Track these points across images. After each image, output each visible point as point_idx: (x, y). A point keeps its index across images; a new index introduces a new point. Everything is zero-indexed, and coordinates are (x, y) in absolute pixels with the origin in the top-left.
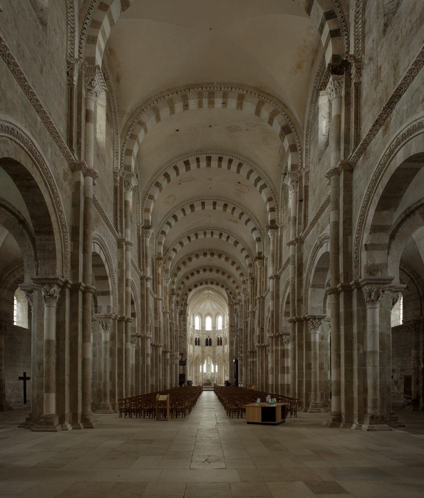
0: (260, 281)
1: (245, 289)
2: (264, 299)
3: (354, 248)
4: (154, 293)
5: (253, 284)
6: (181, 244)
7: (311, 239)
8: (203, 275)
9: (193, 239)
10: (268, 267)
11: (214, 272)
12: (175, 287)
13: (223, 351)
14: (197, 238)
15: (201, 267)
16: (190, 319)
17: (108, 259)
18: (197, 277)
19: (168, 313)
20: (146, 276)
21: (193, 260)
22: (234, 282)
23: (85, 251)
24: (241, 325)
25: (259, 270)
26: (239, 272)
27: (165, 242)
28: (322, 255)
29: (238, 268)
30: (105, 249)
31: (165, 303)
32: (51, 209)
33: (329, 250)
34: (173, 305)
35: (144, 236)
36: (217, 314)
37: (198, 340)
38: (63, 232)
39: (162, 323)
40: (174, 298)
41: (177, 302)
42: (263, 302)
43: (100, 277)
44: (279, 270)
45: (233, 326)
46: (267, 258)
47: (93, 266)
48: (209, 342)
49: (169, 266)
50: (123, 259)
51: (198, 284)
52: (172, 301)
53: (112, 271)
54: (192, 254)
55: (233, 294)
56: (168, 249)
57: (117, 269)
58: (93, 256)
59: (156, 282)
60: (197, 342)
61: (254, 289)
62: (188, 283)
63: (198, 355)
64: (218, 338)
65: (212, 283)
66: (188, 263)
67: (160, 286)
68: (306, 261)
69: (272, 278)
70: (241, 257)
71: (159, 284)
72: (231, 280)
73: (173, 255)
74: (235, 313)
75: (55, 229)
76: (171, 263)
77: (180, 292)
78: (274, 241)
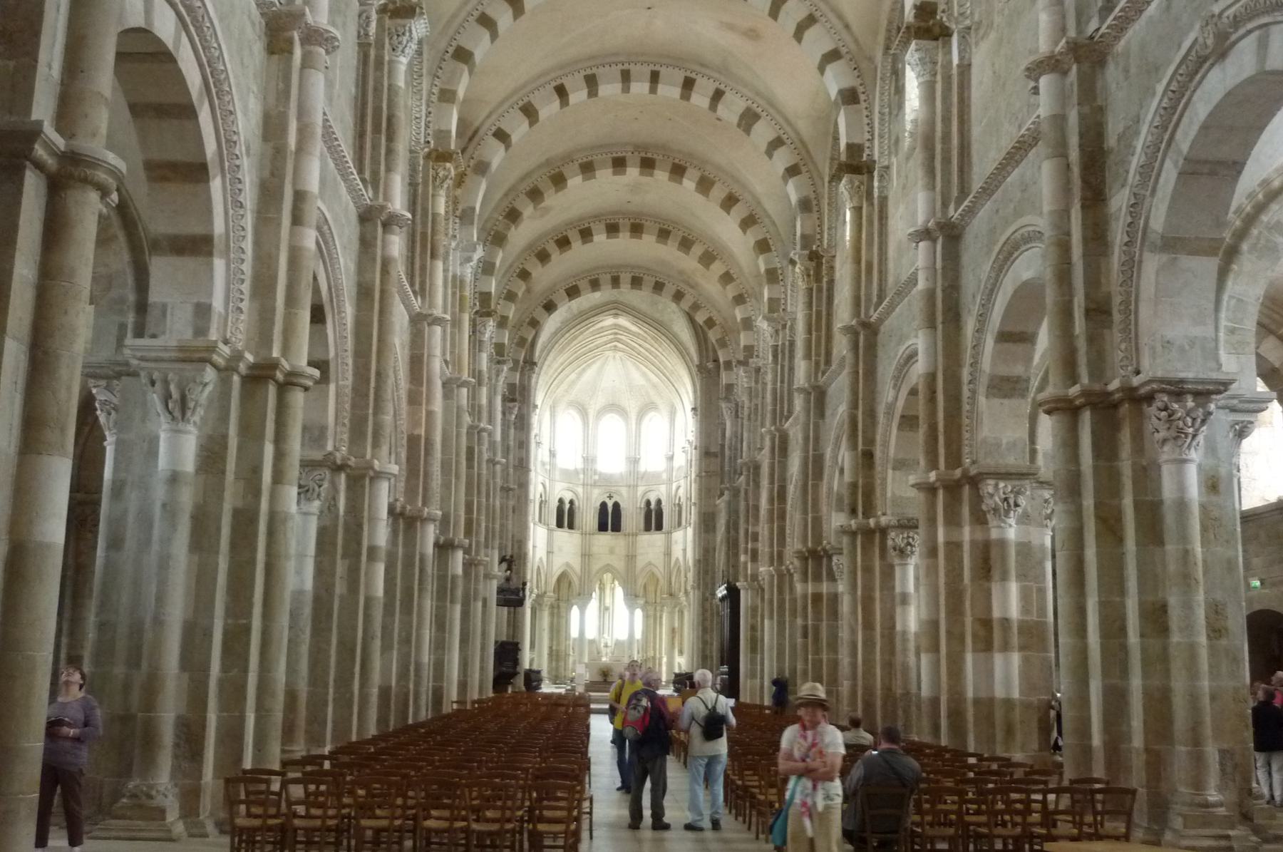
0: (857, 261)
4: (414, 292)
5: (818, 279)
6: (530, 112)
8: (604, 248)
9: (578, 96)
10: (891, 203)
11: (649, 239)
13: (668, 553)
14: (593, 92)
15: (597, 217)
16: (540, 422)
18: (580, 255)
19: (464, 384)
20: (383, 208)
21: (570, 182)
22: (727, 278)
26: (752, 237)
28: (1229, 94)
30: (199, 29)
31: (453, 345)
34: (484, 358)
35: (387, 46)
36: (647, 407)
37: (567, 506)
41: (499, 348)
42: (872, 348)
44: (959, 202)
45: (715, 455)
46: (887, 167)
48: (609, 519)
49: (479, 195)
52: (481, 342)
53: (232, 143)
54: (568, 158)
56: (476, 132)
57: (256, 145)
59: (424, 246)
60: (566, 517)
61: (819, 299)
62: (544, 276)
63: (567, 564)
64: (648, 503)
65: (636, 282)
66: (552, 199)
67: (440, 265)
71: (433, 256)
72: (718, 268)
73: (496, 155)
74: (727, 399)
76: (483, 186)
77: (511, 311)
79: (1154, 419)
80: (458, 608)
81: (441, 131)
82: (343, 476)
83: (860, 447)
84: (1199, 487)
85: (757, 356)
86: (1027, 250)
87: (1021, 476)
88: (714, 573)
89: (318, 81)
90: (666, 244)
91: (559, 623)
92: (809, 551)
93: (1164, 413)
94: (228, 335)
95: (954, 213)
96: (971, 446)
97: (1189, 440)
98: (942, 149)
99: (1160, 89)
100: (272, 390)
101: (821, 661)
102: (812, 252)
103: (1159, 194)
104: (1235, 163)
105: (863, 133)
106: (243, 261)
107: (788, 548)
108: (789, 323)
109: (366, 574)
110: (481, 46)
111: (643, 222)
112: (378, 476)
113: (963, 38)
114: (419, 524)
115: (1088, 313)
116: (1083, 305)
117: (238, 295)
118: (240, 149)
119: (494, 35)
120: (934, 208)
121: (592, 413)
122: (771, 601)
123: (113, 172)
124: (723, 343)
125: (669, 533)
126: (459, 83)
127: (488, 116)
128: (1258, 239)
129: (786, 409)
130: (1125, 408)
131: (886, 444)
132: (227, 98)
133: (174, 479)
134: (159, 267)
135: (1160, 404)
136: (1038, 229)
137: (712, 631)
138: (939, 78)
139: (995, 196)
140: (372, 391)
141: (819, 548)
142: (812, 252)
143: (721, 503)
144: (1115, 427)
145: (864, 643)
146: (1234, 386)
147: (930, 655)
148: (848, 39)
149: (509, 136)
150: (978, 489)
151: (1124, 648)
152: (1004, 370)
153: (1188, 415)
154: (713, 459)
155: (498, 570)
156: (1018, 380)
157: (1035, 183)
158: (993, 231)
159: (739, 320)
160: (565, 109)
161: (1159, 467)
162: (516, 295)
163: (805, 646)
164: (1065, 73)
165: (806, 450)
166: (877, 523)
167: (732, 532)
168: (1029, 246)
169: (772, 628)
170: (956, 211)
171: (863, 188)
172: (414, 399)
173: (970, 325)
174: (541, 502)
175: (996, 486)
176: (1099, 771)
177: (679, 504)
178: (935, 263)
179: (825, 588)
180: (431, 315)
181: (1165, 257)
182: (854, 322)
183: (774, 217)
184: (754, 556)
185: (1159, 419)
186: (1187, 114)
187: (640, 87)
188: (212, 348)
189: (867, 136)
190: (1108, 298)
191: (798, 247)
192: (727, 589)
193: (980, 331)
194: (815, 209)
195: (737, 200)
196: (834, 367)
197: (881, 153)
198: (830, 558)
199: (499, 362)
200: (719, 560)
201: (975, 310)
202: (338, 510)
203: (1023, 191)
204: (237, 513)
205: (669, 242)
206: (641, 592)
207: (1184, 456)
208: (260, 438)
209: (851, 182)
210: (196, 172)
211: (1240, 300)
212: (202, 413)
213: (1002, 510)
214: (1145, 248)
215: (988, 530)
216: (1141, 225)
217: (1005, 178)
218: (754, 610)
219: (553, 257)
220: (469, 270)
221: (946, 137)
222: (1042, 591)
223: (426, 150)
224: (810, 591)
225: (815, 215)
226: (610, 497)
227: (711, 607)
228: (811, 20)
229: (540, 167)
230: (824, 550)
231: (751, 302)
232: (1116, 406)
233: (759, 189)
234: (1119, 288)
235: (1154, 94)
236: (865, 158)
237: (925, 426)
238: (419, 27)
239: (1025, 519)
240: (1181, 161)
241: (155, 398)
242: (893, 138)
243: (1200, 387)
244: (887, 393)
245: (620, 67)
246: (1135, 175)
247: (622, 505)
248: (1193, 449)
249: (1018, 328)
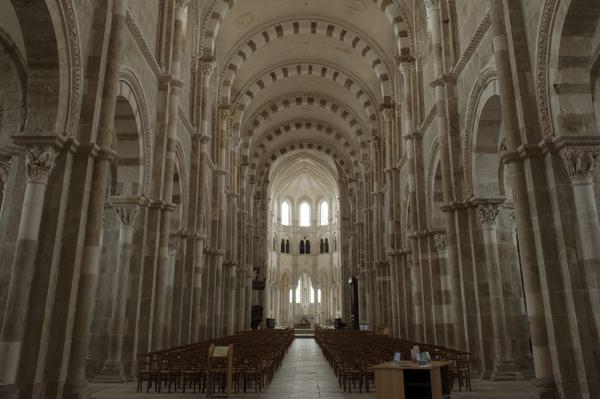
1: (365, 157)
2: (398, 172)
3: (538, 91)
5: (379, 147)
6: (260, 84)
7: (468, 76)
9: (280, 76)
11: (314, 129)
12: (248, 152)
13: (331, 263)
15: (292, 121)
17: (141, 106)
18: (285, 136)
20: (200, 135)
22: (347, 144)
23: (106, 94)
24: (360, 216)
25: (387, 125)
26: (354, 129)
27: (234, 81)
32: (58, 32)
33: (498, 93)
34: (245, 182)
36: (319, 199)
38: (74, 65)
39: (225, 213)
40: (247, 171)
41: (252, 177)
42: (397, 178)
43: (127, 135)
45: (347, 219)
47: (116, 117)
48: (305, 248)
49: (240, 118)
51: (288, 148)
53: (146, 125)
57: (155, 124)
58: (118, 102)
59: (218, 143)
60: (285, 248)
62: (270, 146)
65: (310, 146)
66: (272, 115)
67: (224, 150)
68: (464, 109)
69: (409, 137)
70: (357, 105)
71: (221, 147)
72: (342, 141)
73: (247, 101)
75: (63, 60)
77: (257, 162)
78: (409, 79)
82: (185, 240)
89: (177, 99)
100: (159, 212)
110: (239, 63)
112: (199, 239)
113: (419, 62)
115: (455, 174)
119: (245, 59)
121: (296, 200)
123: (113, 155)
125: (332, 254)
130: (469, 209)
133: (125, 246)
134: (121, 170)
143: (350, 241)
148: (382, 54)
155: (253, 274)
165: (378, 220)
172: (214, 205)
176: (400, 337)
181: (478, 154)
184: (363, 265)
187: (305, 72)
204: (146, 257)
206: (320, 281)
210: (134, 137)
221: (415, 99)
228: (368, 48)
232: (466, 209)
238: (214, 65)
241: (119, 218)
244: (403, 198)
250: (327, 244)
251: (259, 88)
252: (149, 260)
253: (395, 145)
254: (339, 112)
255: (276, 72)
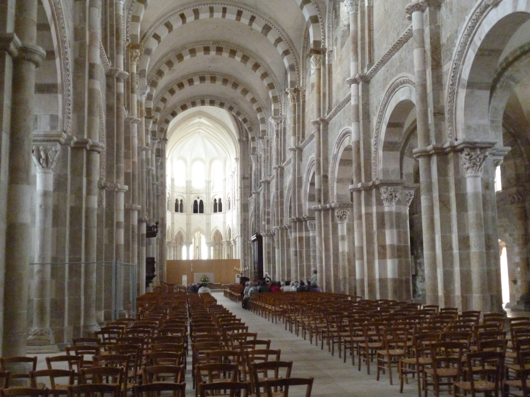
0: (319, 92)
5: (298, 101)
6: (169, 26)
9: (190, 19)
11: (219, 83)
13: (225, 223)
14: (197, 17)
15: (195, 74)
18: (187, 91)
22: (253, 100)
29: (265, 75)
37: (179, 203)
44: (369, 66)
45: (247, 178)
46: (332, 51)
48: (198, 208)
50: (85, 21)
51: (188, 104)
53: (64, 42)
54: (184, 47)
55: (248, 122)
56: (144, 36)
60: (179, 207)
61: (299, 110)
63: (181, 228)
64: (215, 200)
72: (248, 97)
74: (253, 154)
76: (149, 60)
77: (158, 116)
79: (463, 159)
80: (145, 248)
81: (134, 35)
82: (104, 191)
83: (322, 173)
84: (482, 186)
85: (268, 135)
86: (403, 87)
87: (397, 184)
88: (248, 230)
90: (226, 85)
91: (177, 255)
92: (297, 219)
93: (468, 157)
94: (65, 129)
95: (366, 72)
96: (376, 172)
97: (478, 167)
98: (361, 44)
99: (467, 18)
101: (303, 266)
102: (295, 89)
103: (466, 64)
104: (498, 50)
105: (320, 36)
106: (69, 95)
107: (285, 218)
108: (283, 120)
109: (116, 234)
111: (216, 76)
112: (120, 190)
114: (131, 212)
115: (435, 114)
116: (433, 111)
117: (68, 111)
118: (67, 45)
120: (358, 69)
122: (278, 241)
124: (251, 129)
125: (225, 213)
126: (141, 13)
127: (150, 28)
128: (503, 82)
129: (282, 158)
130: (451, 155)
131: (333, 172)
132: (61, 21)
135: (466, 153)
136: (408, 78)
137: (248, 255)
138: (359, 12)
139: (385, 65)
140: (115, 153)
141: (301, 218)
142: (295, 89)
144: (446, 162)
145: (326, 257)
146: (495, 145)
147: (359, 261)
149: (160, 37)
150: (379, 190)
151: (451, 255)
152: (390, 140)
153: (478, 157)
154: (246, 180)
156: (396, 143)
157: (406, 58)
158: (386, 80)
159: (259, 118)
160: (185, 25)
161: (466, 179)
162: (160, 109)
163: (296, 259)
164: (423, 11)
166: (330, 206)
167: (257, 212)
168: (403, 86)
169: (279, 252)
170: (368, 71)
171: (321, 60)
173: (374, 120)
174: (168, 201)
175: (387, 189)
177: (229, 201)
178: (358, 93)
179: (304, 234)
180: (133, 119)
181: (469, 91)
182: (318, 119)
183: (276, 73)
184: (268, 222)
185: (466, 159)
186: (479, 29)
187: (218, 15)
188: (60, 136)
189: (322, 37)
190: (443, 107)
191: (289, 87)
192: (256, 236)
193: (379, 122)
194: (296, 69)
195: (259, 66)
196: (307, 138)
197: (329, 45)
198: (306, 221)
199: (154, 139)
200: (250, 225)
201: (377, 113)
202: (103, 206)
203: (400, 62)
204: (72, 208)
205: (228, 85)
207: (476, 175)
208: (81, 175)
209: (316, 58)
211: (496, 109)
212: (55, 164)
213: (390, 199)
214: (459, 87)
215: (384, 207)
216: (458, 77)
217: (392, 56)
218: (269, 245)
219: (176, 92)
220: (144, 98)
221: (363, 38)
222: (406, 233)
223: (127, 44)
224: (298, 236)
225: (296, 72)
226: (198, 198)
227: (248, 244)
229: (172, 51)
230: (303, 218)
231: (264, 111)
232: (447, 154)
233: (269, 60)
234: (448, 104)
235: (465, 20)
236: (321, 47)
237: (356, 164)
239: (399, 203)
240: (477, 50)
241: (34, 159)
242: (334, 38)
243: (483, 146)
245: (209, 5)
246: (455, 55)
247: (204, 202)
248: (479, 172)
249: (396, 121)
250: (220, 205)
251: (167, 30)
252: (76, 212)
253: (324, 94)
254: (250, 64)
255: (185, 12)
